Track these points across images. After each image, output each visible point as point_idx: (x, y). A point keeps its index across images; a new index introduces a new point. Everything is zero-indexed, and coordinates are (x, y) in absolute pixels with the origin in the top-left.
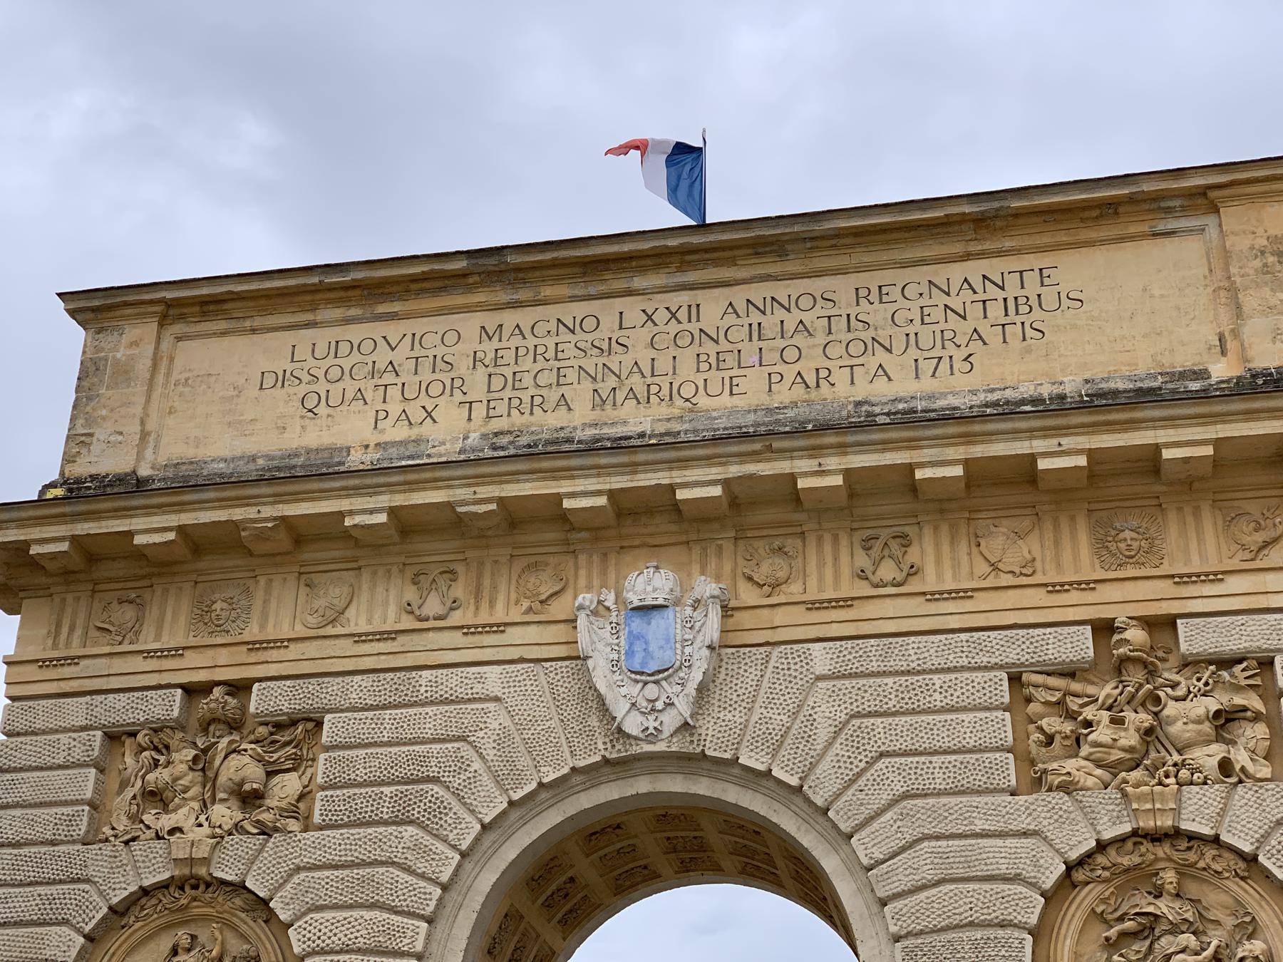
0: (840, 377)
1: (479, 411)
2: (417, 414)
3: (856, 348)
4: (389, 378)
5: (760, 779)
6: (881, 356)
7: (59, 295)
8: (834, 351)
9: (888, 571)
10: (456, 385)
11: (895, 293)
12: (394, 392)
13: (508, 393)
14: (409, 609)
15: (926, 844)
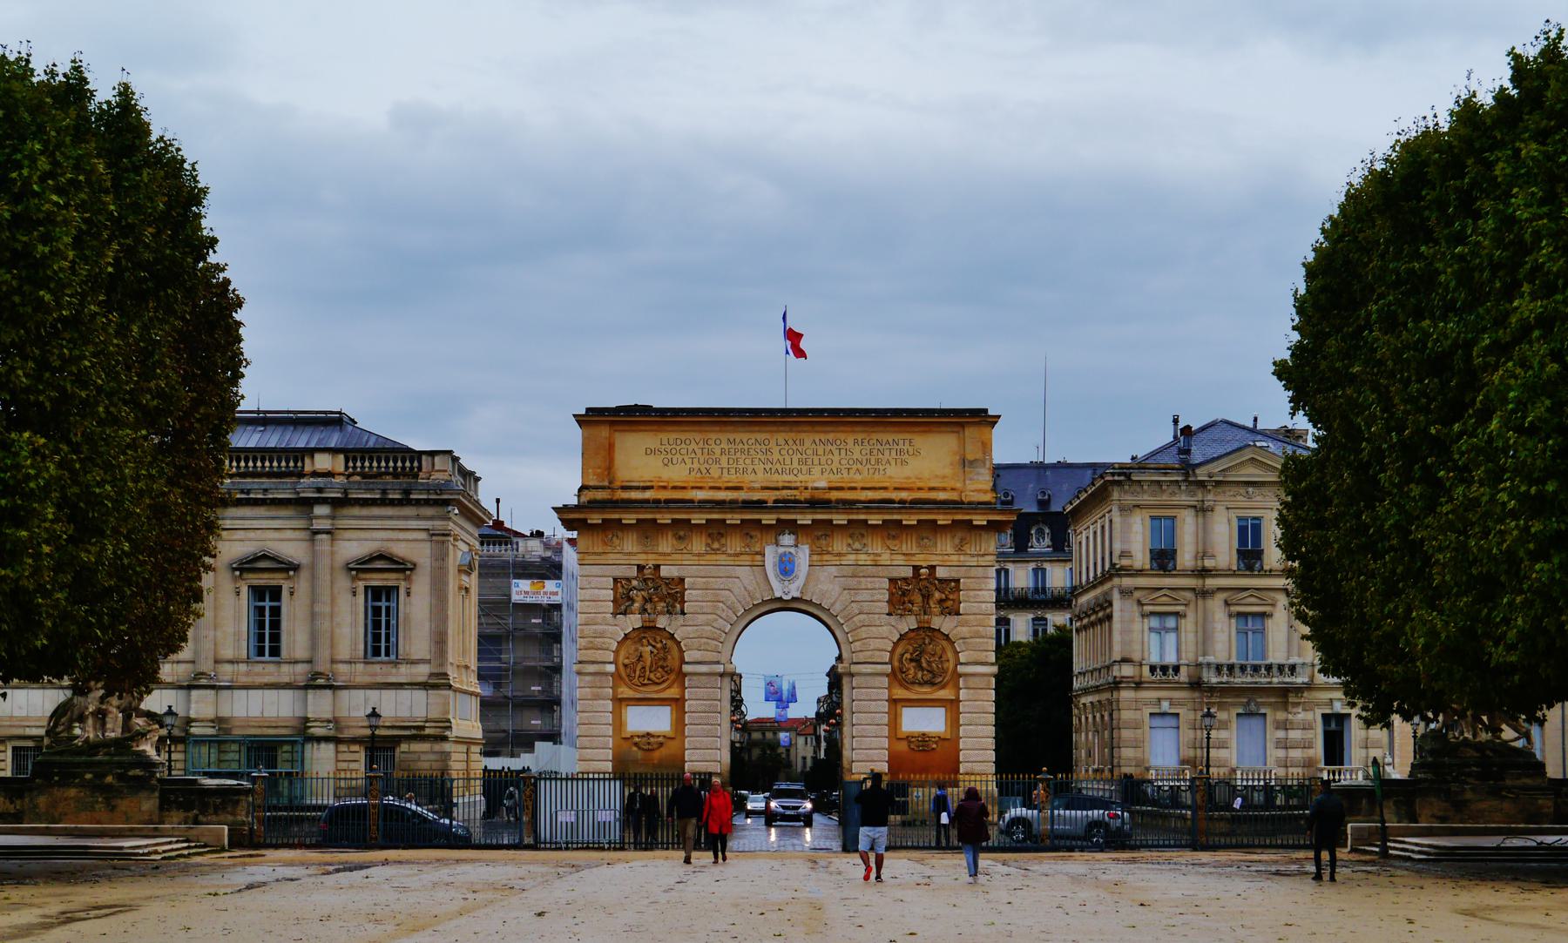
0: (845, 472)
1: (725, 471)
2: (704, 471)
3: (851, 462)
4: (693, 455)
5: (819, 606)
6: (859, 466)
7: (574, 415)
8: (843, 462)
9: (857, 545)
10: (717, 461)
11: (866, 441)
12: (696, 461)
13: (735, 466)
14: (708, 545)
15: (863, 629)
